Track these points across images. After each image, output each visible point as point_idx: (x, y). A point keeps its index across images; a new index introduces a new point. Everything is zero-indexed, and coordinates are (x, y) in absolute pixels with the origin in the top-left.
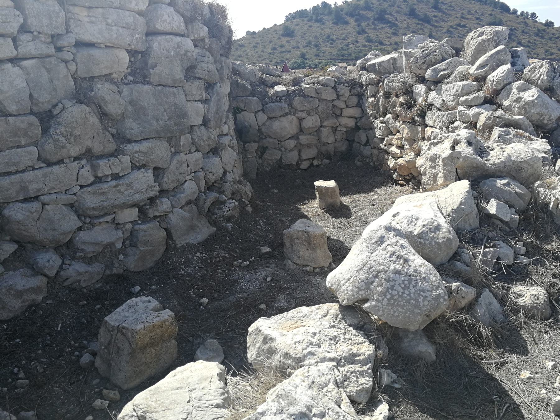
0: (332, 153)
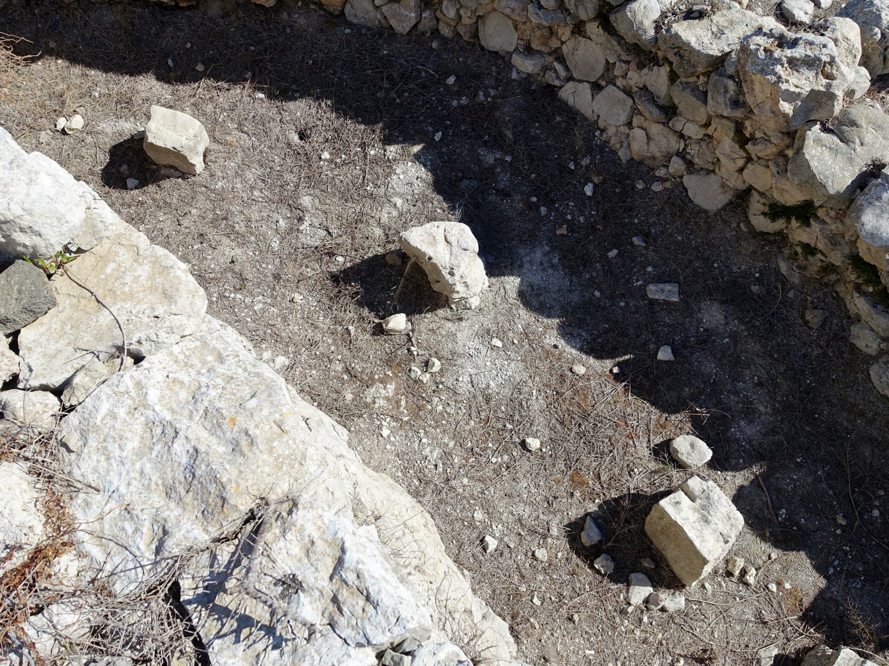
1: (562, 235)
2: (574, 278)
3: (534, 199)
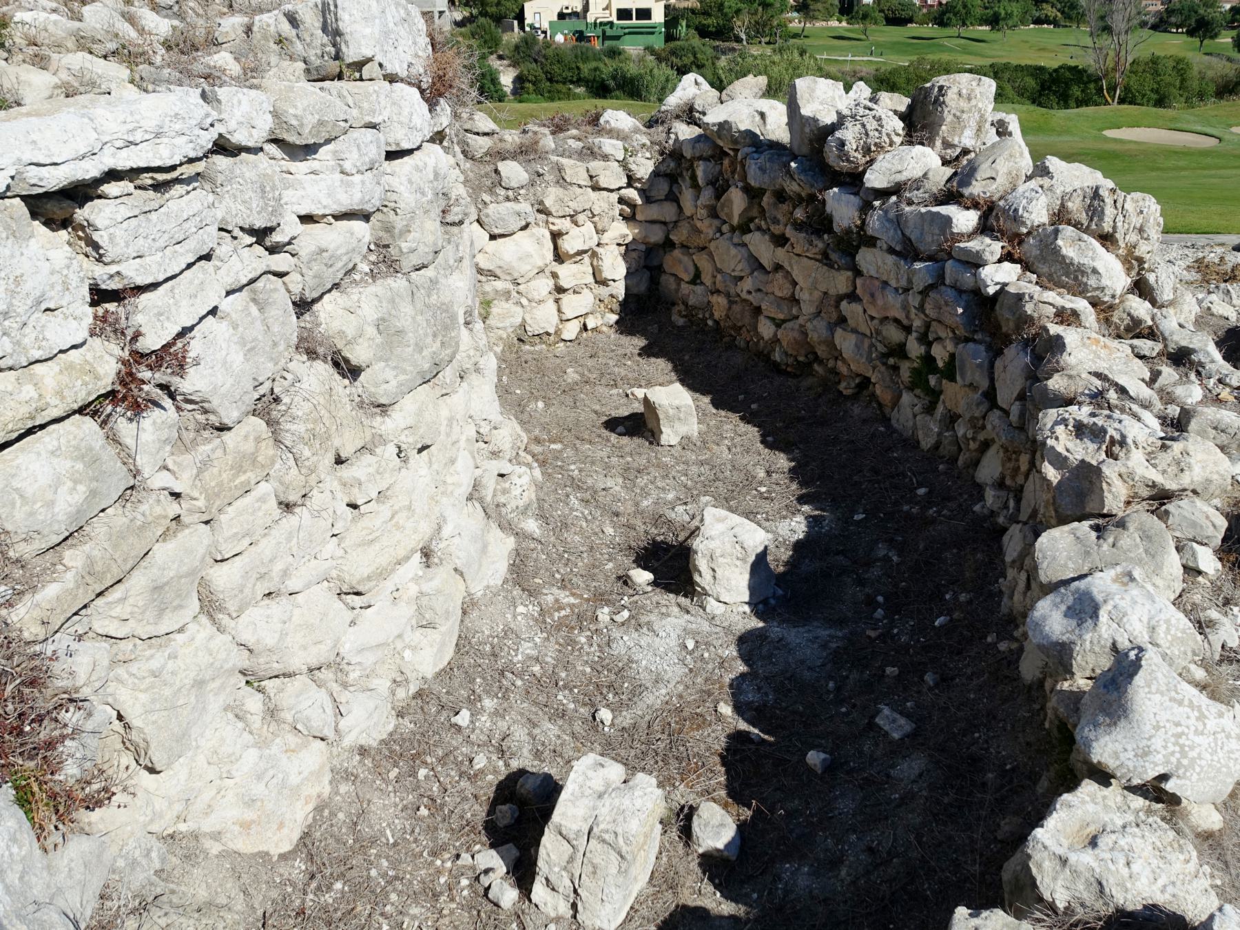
1: (869, 637)
2: (829, 666)
3: (880, 599)
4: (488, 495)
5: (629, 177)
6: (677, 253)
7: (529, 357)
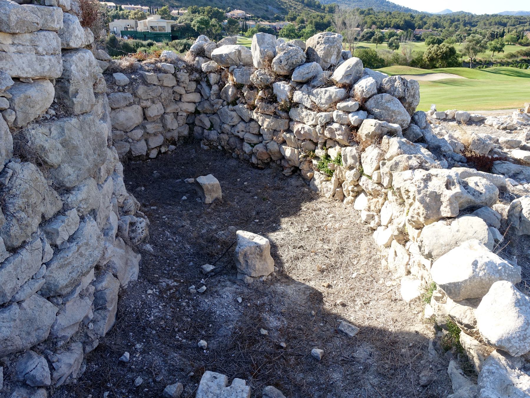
0: (176, 139)
4: (126, 234)
5: (178, 81)
6: (202, 116)
7: (134, 167)
